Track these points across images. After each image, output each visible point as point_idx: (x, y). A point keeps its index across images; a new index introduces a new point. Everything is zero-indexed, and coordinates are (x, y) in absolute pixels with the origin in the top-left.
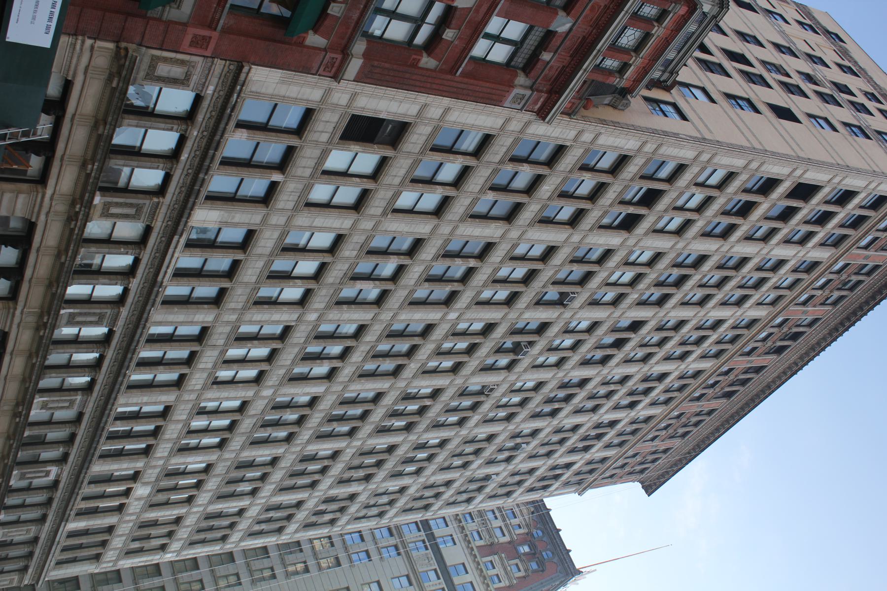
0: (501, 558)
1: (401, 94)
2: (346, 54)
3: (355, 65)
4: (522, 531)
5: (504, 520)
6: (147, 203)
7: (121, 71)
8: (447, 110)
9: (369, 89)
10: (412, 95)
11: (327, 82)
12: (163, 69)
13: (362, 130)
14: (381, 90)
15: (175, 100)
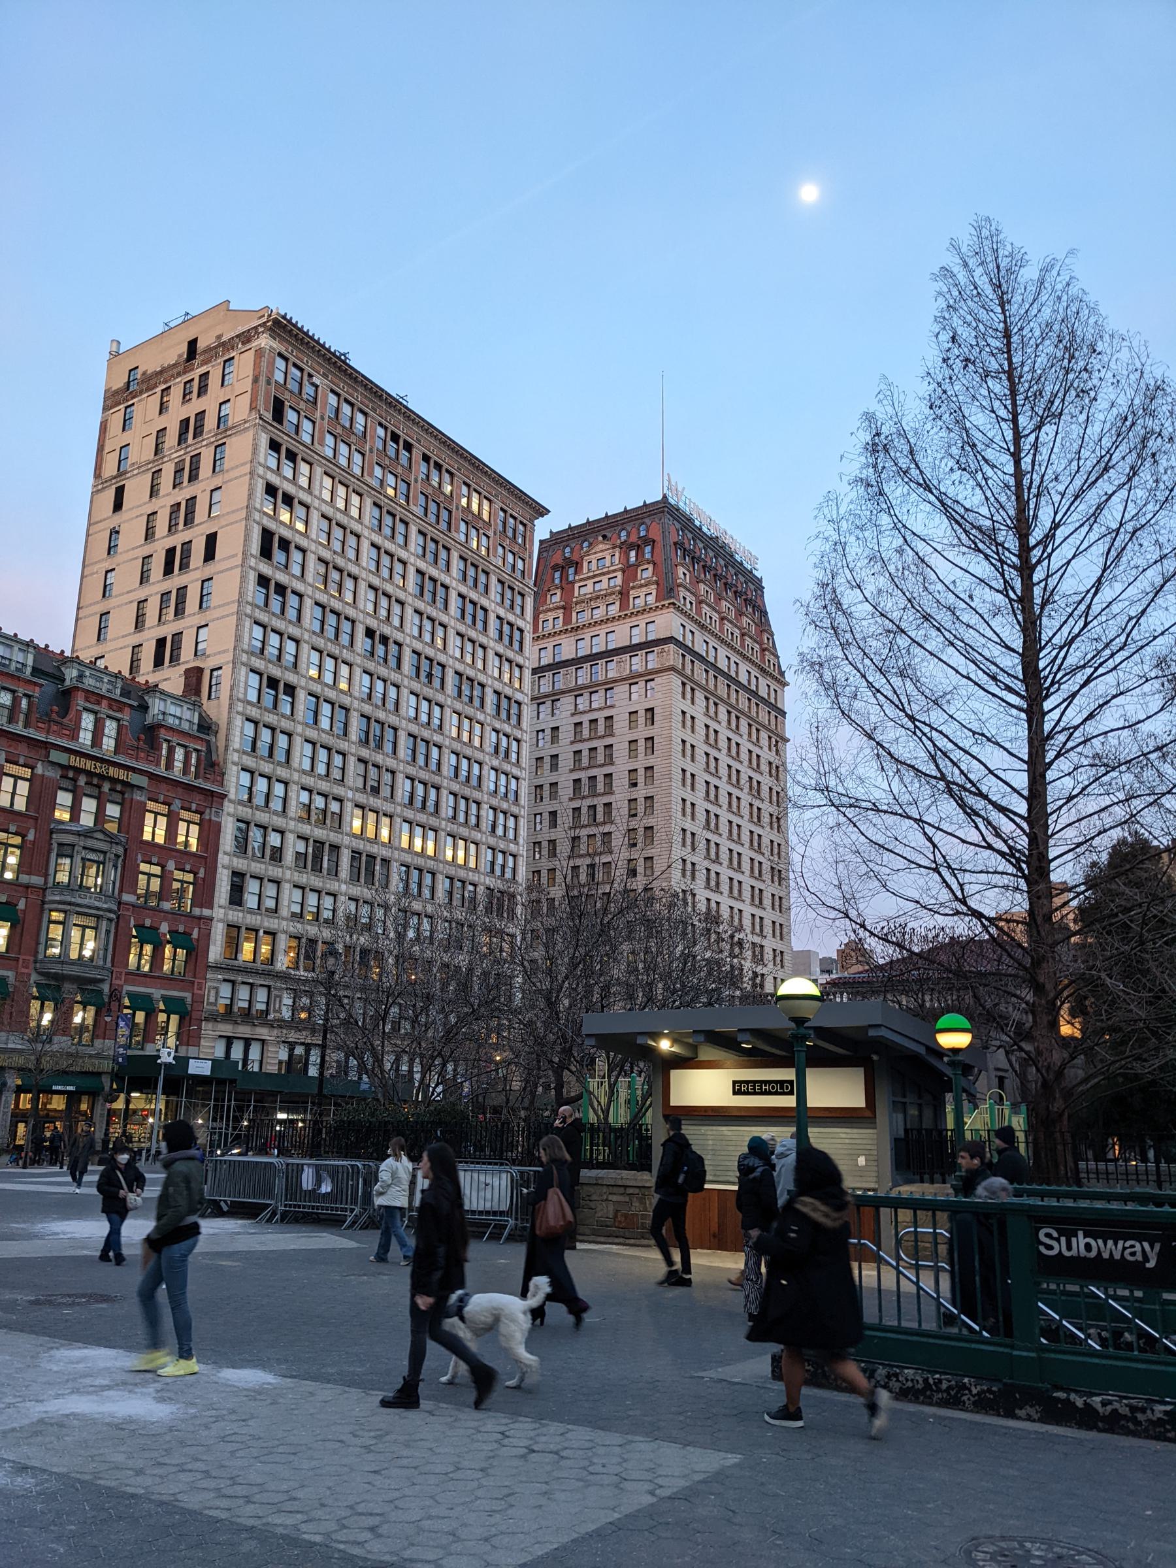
0: (633, 588)
1: (218, 882)
2: (200, 918)
3: (206, 912)
4: (617, 555)
5: (604, 574)
6: (274, 992)
7: (214, 1018)
8: (225, 853)
9: (216, 900)
10: (218, 876)
11: (214, 923)
12: (212, 999)
13: (237, 897)
14: (217, 894)
15: (225, 990)
